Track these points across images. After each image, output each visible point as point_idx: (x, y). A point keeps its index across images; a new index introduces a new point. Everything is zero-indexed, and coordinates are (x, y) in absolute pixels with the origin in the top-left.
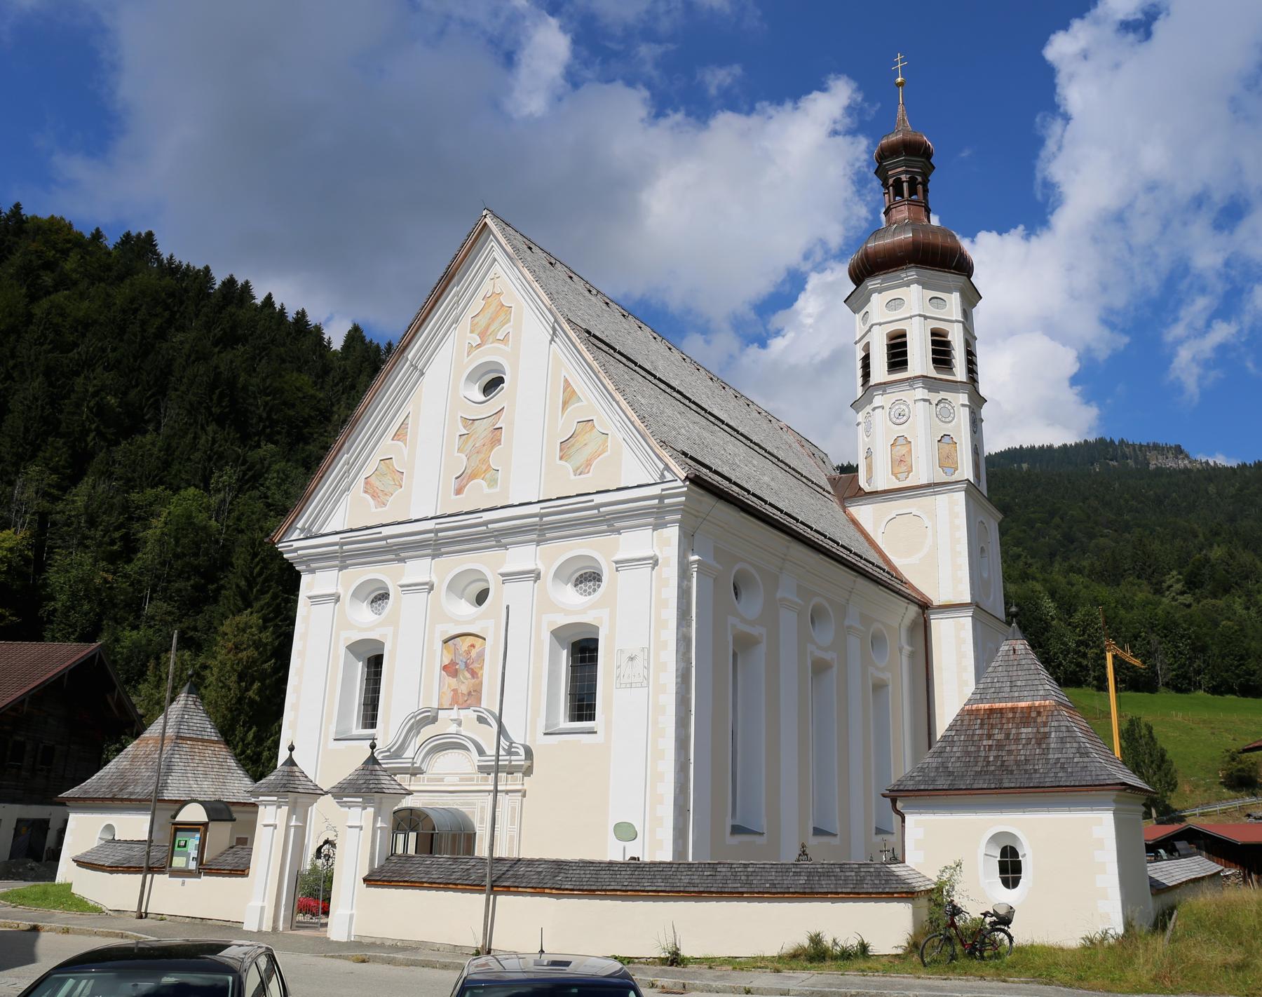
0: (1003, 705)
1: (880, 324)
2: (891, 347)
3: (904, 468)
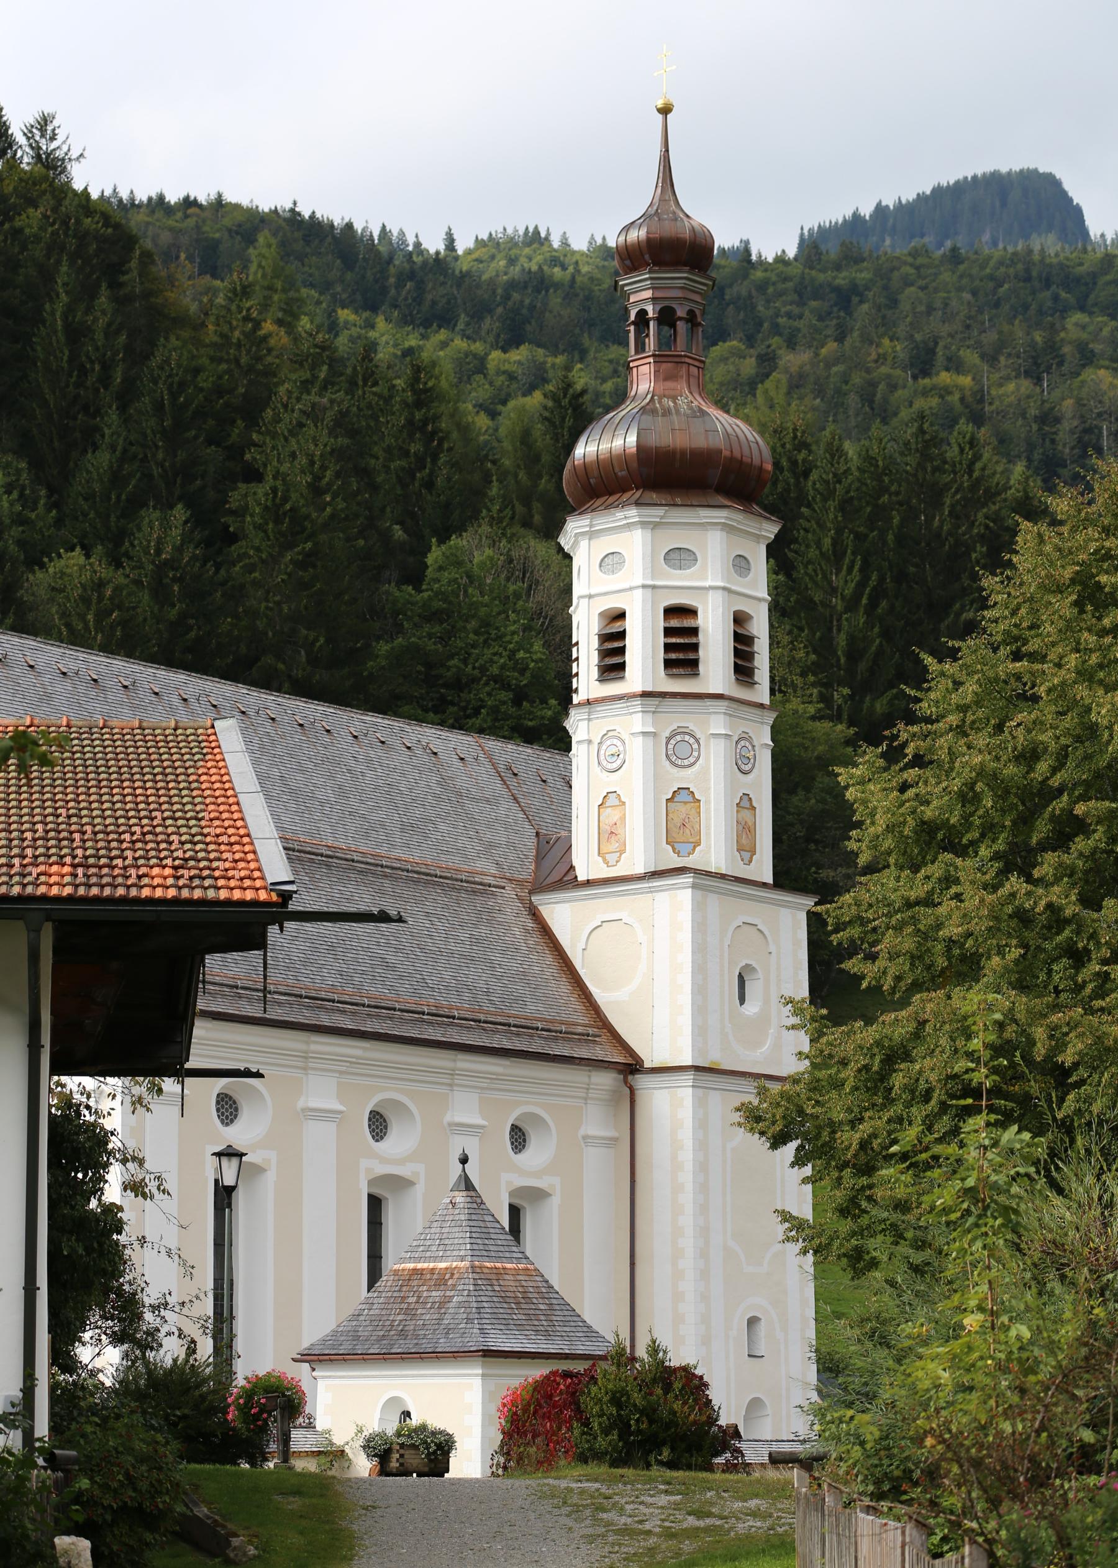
0: (425, 1265)
1: (590, 597)
2: (605, 638)
3: (614, 846)
